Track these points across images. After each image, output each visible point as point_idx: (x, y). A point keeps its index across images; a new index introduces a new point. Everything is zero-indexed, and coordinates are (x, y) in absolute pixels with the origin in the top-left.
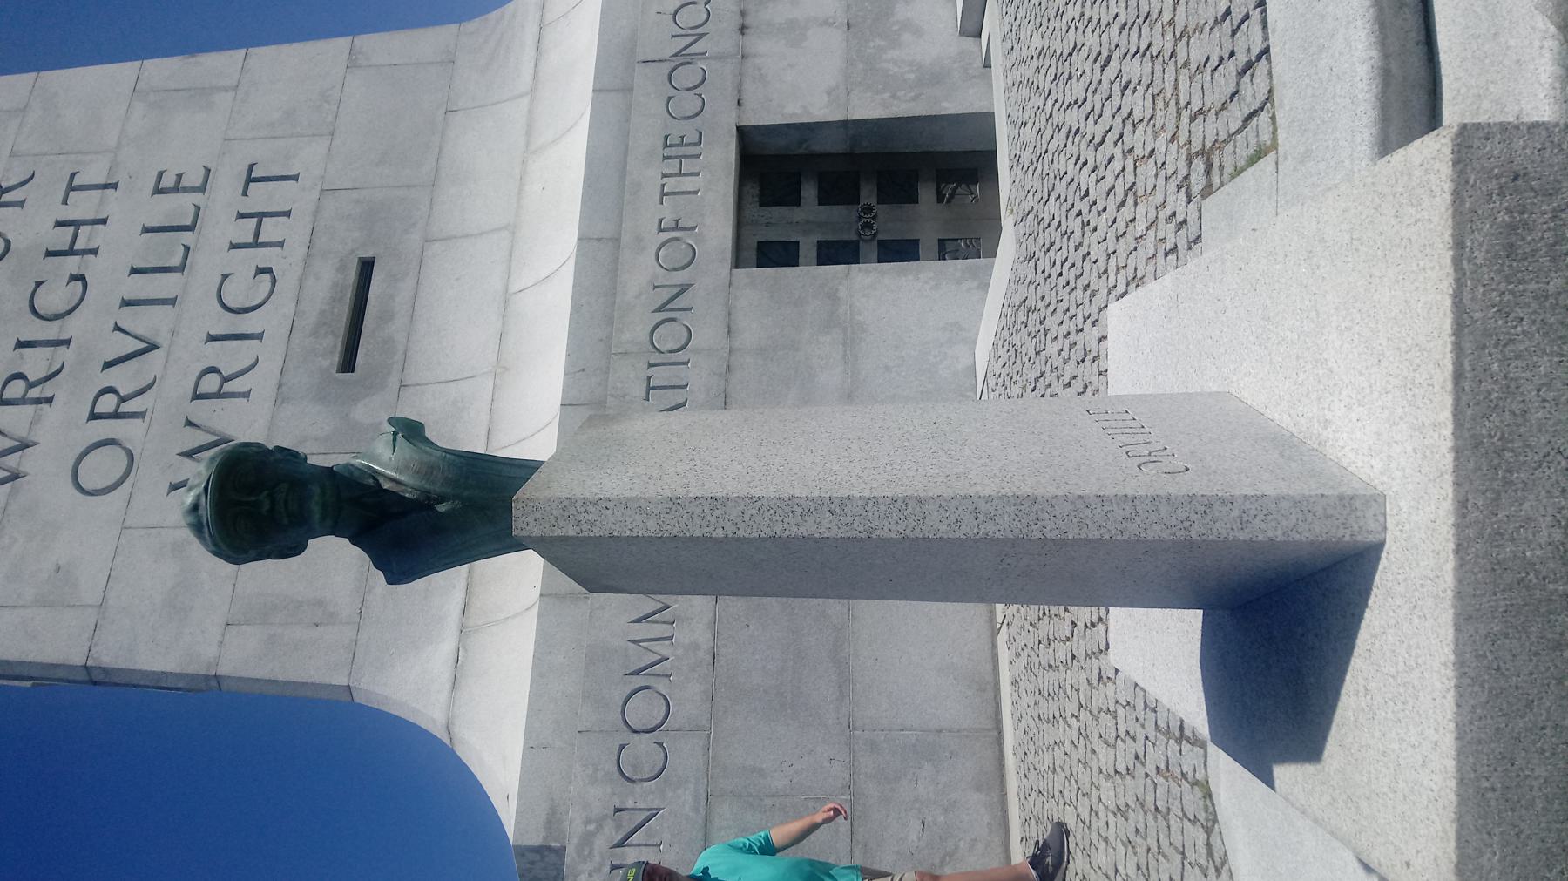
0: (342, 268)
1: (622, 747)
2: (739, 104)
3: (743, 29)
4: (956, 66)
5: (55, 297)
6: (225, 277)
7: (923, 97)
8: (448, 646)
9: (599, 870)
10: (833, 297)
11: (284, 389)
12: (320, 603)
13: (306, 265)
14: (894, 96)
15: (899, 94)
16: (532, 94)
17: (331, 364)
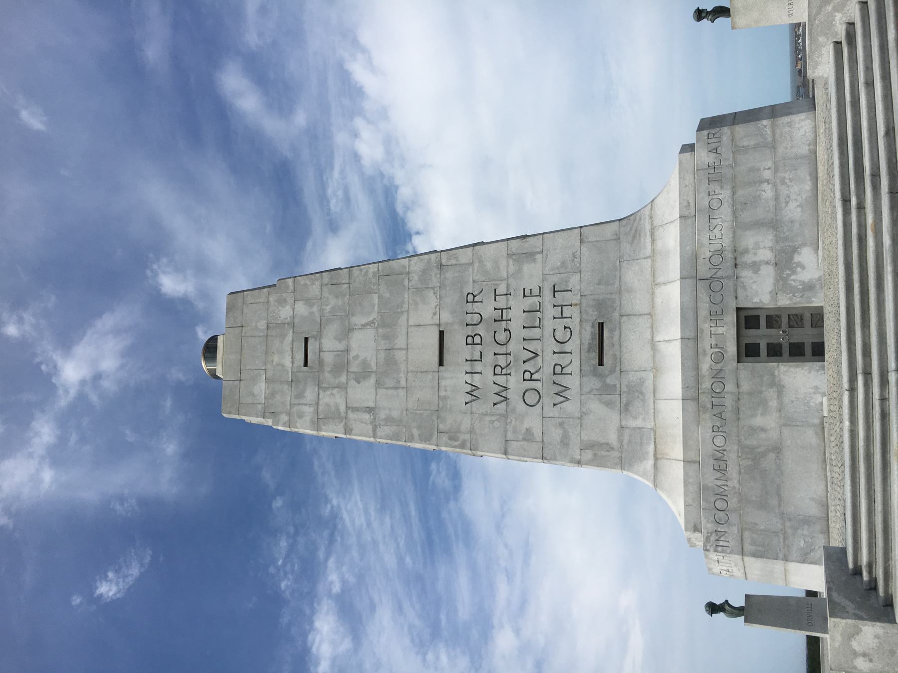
0: (593, 326)
1: (715, 514)
2: (736, 298)
3: (736, 265)
4: (817, 283)
5: (502, 337)
6: (554, 330)
7: (805, 296)
8: (651, 462)
9: (712, 545)
10: (773, 375)
11: (583, 371)
12: (608, 444)
13: (581, 326)
14: (794, 296)
15: (796, 294)
16: (653, 256)
17: (596, 362)
